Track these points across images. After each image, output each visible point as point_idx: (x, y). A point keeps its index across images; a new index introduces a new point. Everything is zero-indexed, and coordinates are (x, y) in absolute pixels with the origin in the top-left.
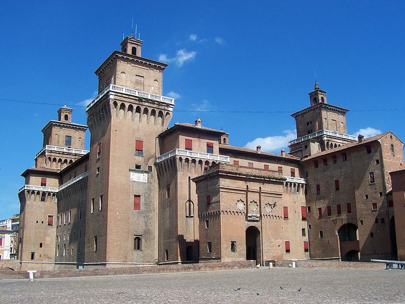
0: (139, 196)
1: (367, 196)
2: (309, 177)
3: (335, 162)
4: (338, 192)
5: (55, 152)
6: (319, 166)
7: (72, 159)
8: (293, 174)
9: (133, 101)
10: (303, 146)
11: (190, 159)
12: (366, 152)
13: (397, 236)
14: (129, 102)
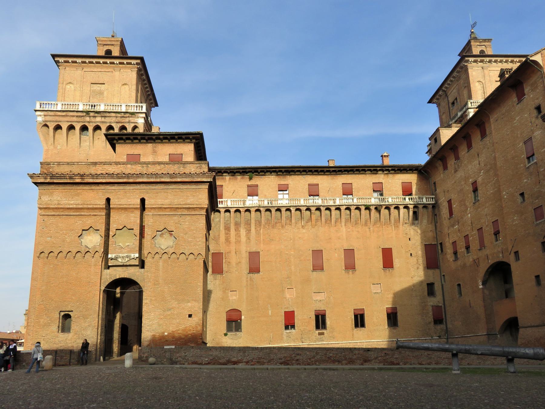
1: (522, 194)
2: (438, 190)
3: (470, 146)
4: (477, 204)
6: (449, 166)
9: (75, 119)
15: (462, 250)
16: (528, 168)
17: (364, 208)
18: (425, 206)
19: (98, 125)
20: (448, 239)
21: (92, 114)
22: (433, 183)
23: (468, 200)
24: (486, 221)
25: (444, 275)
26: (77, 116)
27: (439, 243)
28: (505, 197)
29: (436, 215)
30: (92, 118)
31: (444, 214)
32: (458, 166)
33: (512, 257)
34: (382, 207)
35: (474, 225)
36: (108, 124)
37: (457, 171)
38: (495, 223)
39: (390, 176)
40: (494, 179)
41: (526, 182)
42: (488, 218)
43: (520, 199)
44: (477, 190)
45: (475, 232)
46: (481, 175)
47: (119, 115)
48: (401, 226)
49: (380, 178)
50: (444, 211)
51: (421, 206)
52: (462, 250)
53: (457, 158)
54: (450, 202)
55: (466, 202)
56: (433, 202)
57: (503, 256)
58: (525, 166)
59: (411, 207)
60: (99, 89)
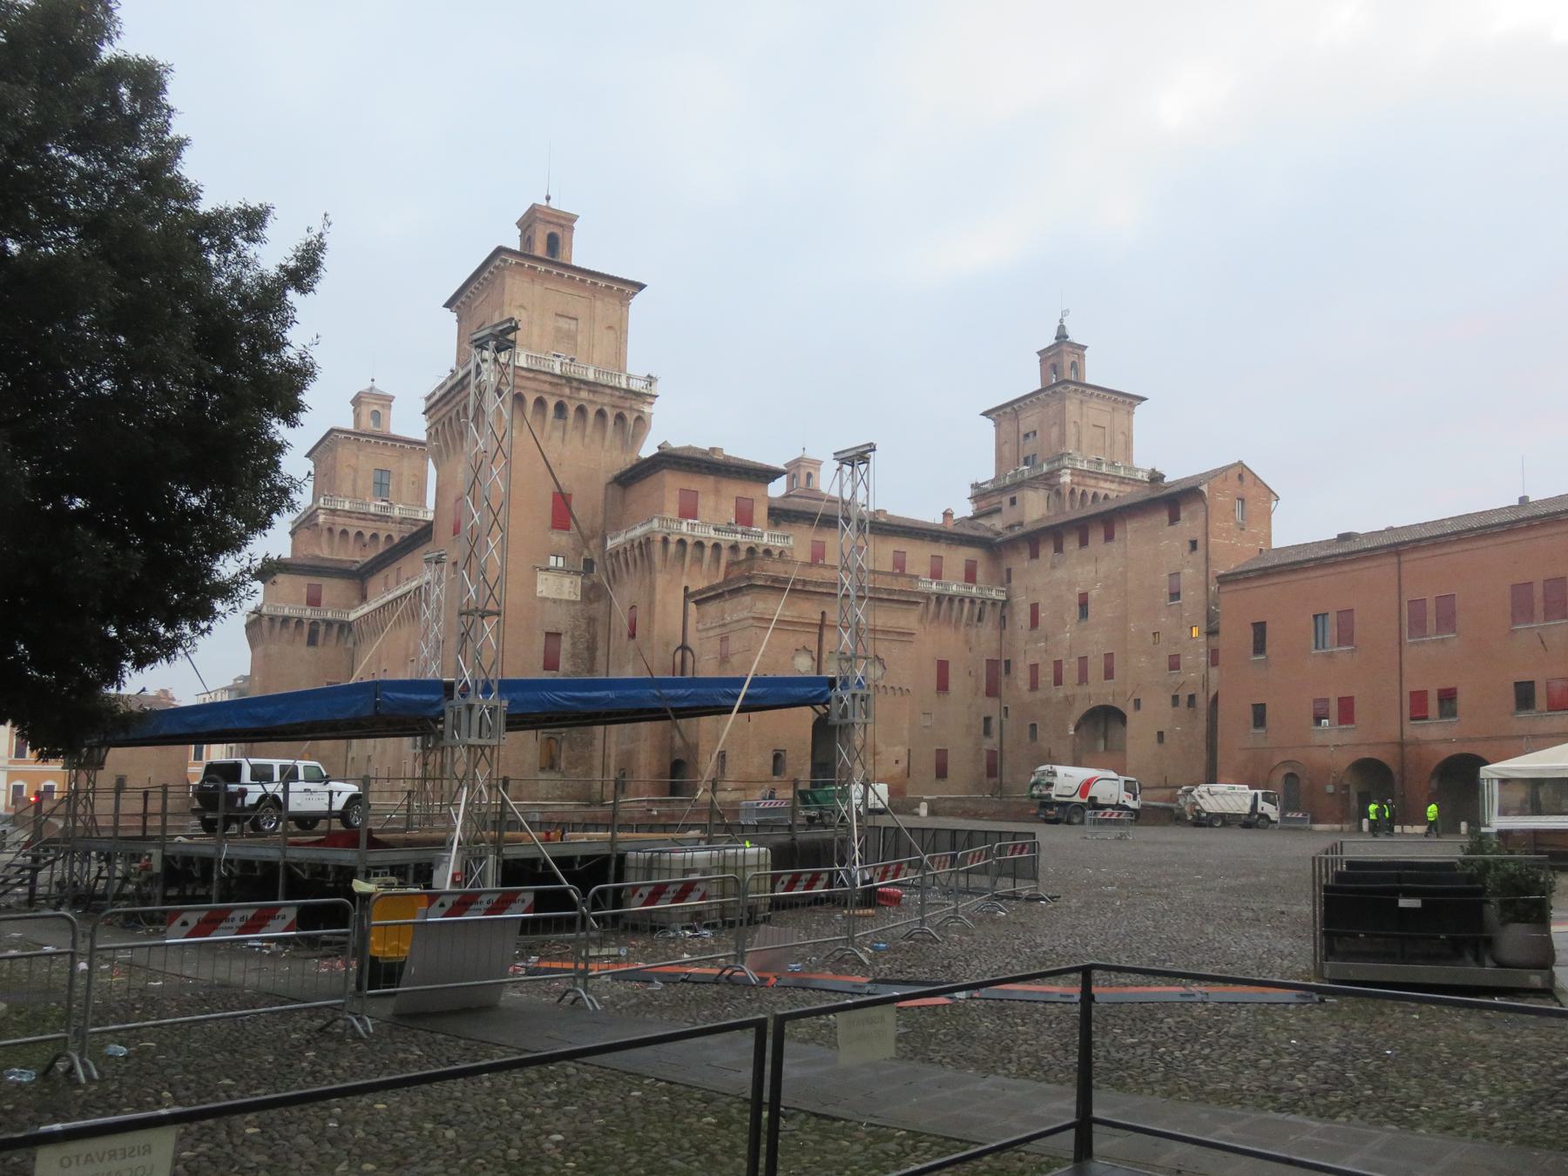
0: (559, 635)
2: (1014, 582)
3: (1084, 542)
5: (348, 514)
6: (1042, 553)
7: (393, 534)
8: (970, 577)
10: (1006, 500)
11: (689, 541)
13: (1219, 740)
14: (537, 391)
15: (1047, 675)
18: (994, 603)
22: (1004, 569)
26: (551, 383)
29: (1004, 617)
33: (1131, 704)
36: (599, 407)
38: (1109, 656)
39: (953, 546)
43: (1151, 639)
45: (1074, 660)
47: (617, 393)
49: (941, 550)
50: (1023, 617)
51: (989, 602)
52: (1047, 675)
53: (1059, 549)
54: (1035, 609)
56: (1004, 598)
57: (1114, 700)
59: (978, 601)
60: (566, 326)
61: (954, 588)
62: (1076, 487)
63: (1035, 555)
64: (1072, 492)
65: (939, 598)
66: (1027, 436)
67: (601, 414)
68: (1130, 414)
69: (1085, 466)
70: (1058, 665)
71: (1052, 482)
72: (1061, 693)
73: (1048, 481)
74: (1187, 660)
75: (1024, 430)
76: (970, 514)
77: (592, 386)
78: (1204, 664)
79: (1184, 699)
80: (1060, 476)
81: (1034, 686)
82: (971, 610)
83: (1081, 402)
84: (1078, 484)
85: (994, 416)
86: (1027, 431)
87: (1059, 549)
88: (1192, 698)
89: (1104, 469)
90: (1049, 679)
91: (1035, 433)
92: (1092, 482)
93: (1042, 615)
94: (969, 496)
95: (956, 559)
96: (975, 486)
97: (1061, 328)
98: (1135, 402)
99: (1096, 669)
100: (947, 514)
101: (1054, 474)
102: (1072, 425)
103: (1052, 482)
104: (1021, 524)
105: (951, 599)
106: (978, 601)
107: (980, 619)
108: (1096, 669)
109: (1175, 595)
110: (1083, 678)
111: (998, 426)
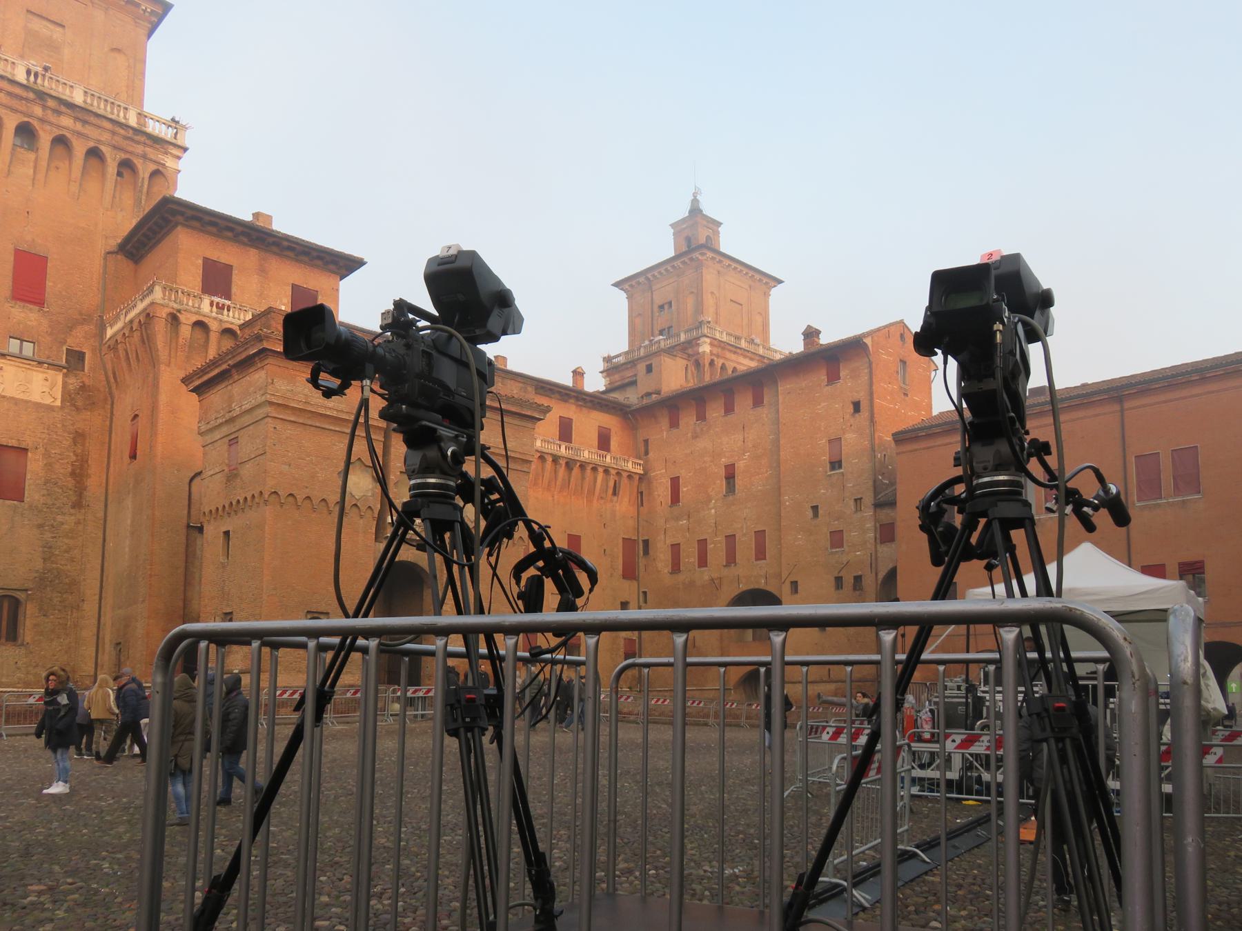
2: (651, 454)
3: (729, 409)
4: (731, 498)
8: (604, 442)
10: (641, 367)
12: (824, 378)
16: (830, 476)
17: (551, 459)
19: (63, 135)
20: (663, 537)
21: (51, 103)
23: (713, 489)
24: (745, 526)
25: (645, 593)
26: (10, 94)
27: (641, 539)
28: (787, 503)
29: (642, 493)
30: (49, 112)
31: (659, 496)
32: (702, 430)
34: (576, 464)
35: (720, 528)
36: (92, 144)
37: (697, 437)
39: (585, 410)
40: (767, 471)
41: (824, 494)
42: (749, 524)
43: (810, 513)
44: (734, 477)
45: (721, 539)
46: (745, 459)
48: (595, 501)
51: (625, 474)
53: (701, 417)
54: (675, 482)
55: (710, 490)
56: (642, 472)
57: (766, 583)
58: (826, 472)
59: (613, 472)
61: (586, 454)
62: (715, 359)
63: (674, 424)
64: (712, 363)
65: (569, 464)
66: (661, 307)
67: (94, 153)
68: (766, 295)
69: (724, 338)
70: (703, 544)
71: (690, 351)
72: (705, 575)
73: (687, 349)
74: (851, 536)
75: (658, 300)
76: (602, 388)
77: (81, 113)
78: (872, 541)
79: (848, 581)
80: (698, 345)
81: (676, 567)
82: (606, 481)
83: (719, 272)
84: (718, 356)
85: (626, 286)
86: (660, 304)
87: (701, 417)
88: (858, 579)
89: (743, 344)
90: (692, 560)
91: (670, 303)
92: (733, 357)
93: (684, 489)
94: (602, 369)
95: (588, 424)
96: (608, 359)
97: (695, 201)
98: (772, 283)
99: (745, 547)
100: (578, 374)
101: (692, 343)
102: (710, 295)
103: (690, 351)
104: (658, 393)
105: (583, 466)
106: (613, 472)
107: (615, 493)
108: (745, 547)
109: (836, 464)
110: (731, 559)
111: (630, 298)
